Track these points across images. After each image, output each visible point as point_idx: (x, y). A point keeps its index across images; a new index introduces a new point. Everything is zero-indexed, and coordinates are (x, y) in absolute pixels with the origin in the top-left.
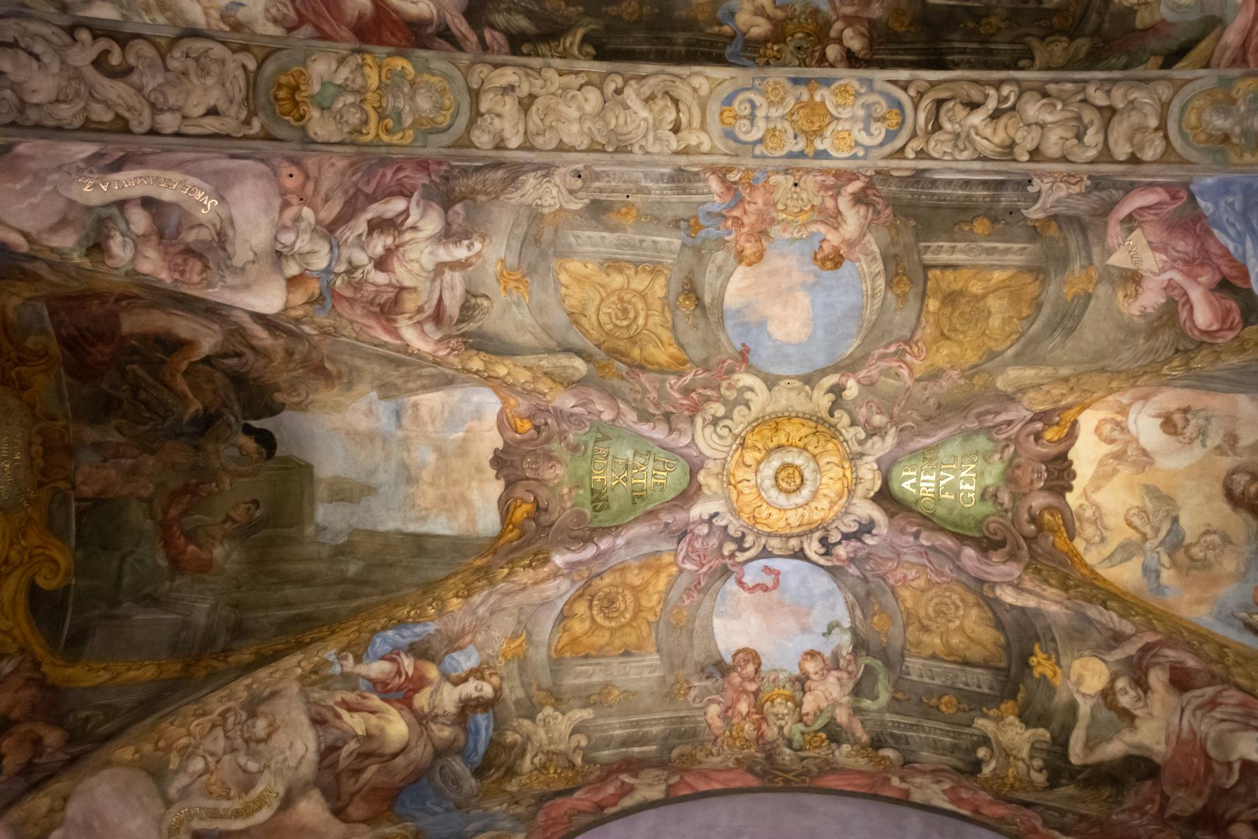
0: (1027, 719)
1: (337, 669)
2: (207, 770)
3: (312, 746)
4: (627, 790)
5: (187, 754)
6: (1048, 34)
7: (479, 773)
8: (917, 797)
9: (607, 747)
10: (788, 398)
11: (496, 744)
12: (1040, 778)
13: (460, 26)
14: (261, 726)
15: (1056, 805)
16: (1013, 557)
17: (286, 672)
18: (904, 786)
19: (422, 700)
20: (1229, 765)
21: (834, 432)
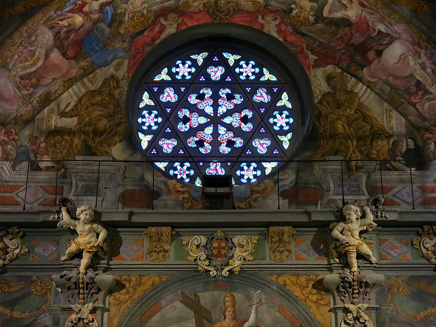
1: (56, 15)
2: (19, 56)
3: (51, 35)
4: (163, 28)
5: (12, 57)
7: (110, 26)
8: (266, 30)
9: (155, 5)
11: (115, 15)
12: (312, 19)
14: (33, 38)
15: (313, 35)
17: (38, 23)
18: (263, 22)
19: (86, 9)
20: (375, 30)
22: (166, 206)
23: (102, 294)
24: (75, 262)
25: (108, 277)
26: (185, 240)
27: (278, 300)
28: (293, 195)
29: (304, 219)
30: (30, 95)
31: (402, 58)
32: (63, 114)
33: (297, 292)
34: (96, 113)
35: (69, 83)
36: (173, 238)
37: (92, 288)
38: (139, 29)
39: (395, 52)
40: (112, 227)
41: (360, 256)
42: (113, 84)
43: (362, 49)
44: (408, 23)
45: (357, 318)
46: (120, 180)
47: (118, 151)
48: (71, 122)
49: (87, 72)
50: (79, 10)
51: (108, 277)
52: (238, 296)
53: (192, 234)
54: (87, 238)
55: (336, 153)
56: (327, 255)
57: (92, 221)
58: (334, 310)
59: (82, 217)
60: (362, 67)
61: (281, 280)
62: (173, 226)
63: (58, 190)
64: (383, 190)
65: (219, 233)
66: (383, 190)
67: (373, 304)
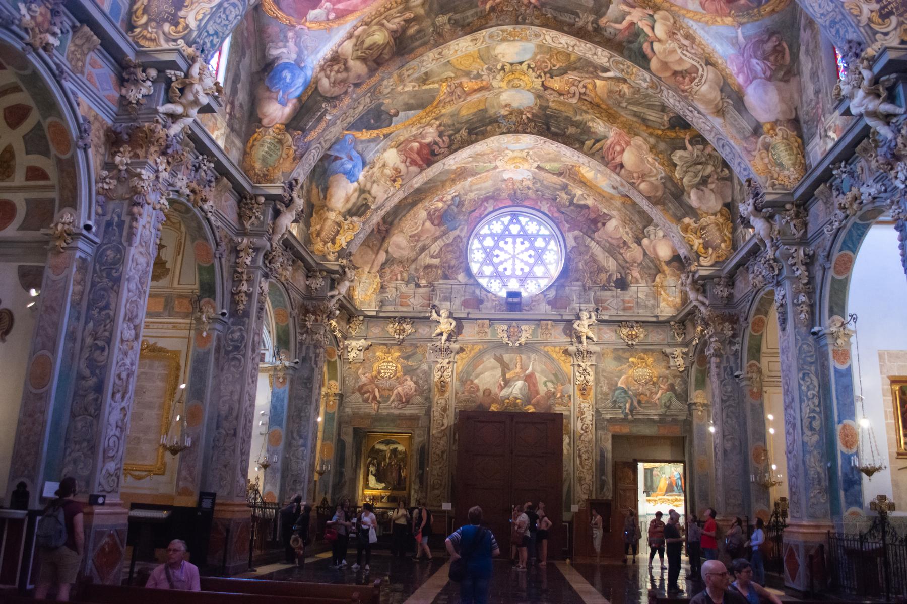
0: (566, 193)
4: (486, 208)
6: (572, 125)
10: (516, 154)
13: (438, 139)
16: (564, 177)
21: (527, 160)
22: (487, 308)
23: (453, 355)
24: (440, 337)
25: (455, 346)
26: (496, 326)
27: (544, 359)
28: (553, 303)
29: (559, 318)
30: (415, 246)
31: (616, 228)
32: (432, 257)
33: (554, 356)
34: (450, 256)
35: (436, 239)
36: (490, 326)
37: (448, 351)
38: (473, 209)
39: (612, 224)
40: (458, 319)
41: (587, 338)
42: (459, 240)
43: (595, 222)
44: (619, 211)
45: (585, 370)
46: (462, 293)
47: (461, 277)
48: (436, 261)
49: (445, 233)
50: (441, 200)
51: (455, 346)
52: (523, 357)
53: (499, 324)
54: (446, 325)
55: (578, 280)
56: (571, 336)
57: (449, 317)
58: (573, 365)
59: (443, 315)
60: (594, 232)
61: (546, 349)
62: (490, 320)
63: (430, 299)
64: (602, 301)
65: (514, 323)
66: (602, 301)
67: (594, 363)
